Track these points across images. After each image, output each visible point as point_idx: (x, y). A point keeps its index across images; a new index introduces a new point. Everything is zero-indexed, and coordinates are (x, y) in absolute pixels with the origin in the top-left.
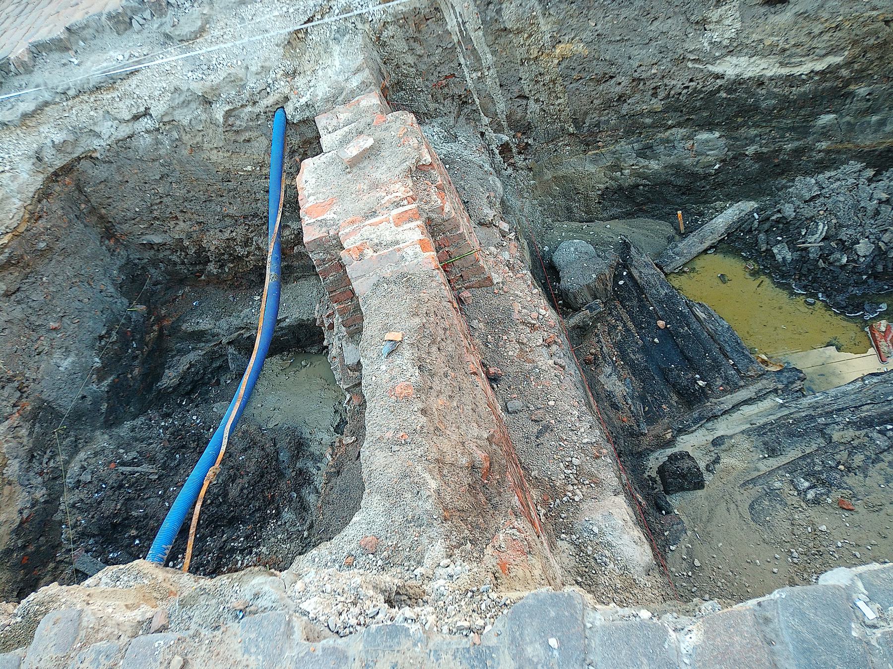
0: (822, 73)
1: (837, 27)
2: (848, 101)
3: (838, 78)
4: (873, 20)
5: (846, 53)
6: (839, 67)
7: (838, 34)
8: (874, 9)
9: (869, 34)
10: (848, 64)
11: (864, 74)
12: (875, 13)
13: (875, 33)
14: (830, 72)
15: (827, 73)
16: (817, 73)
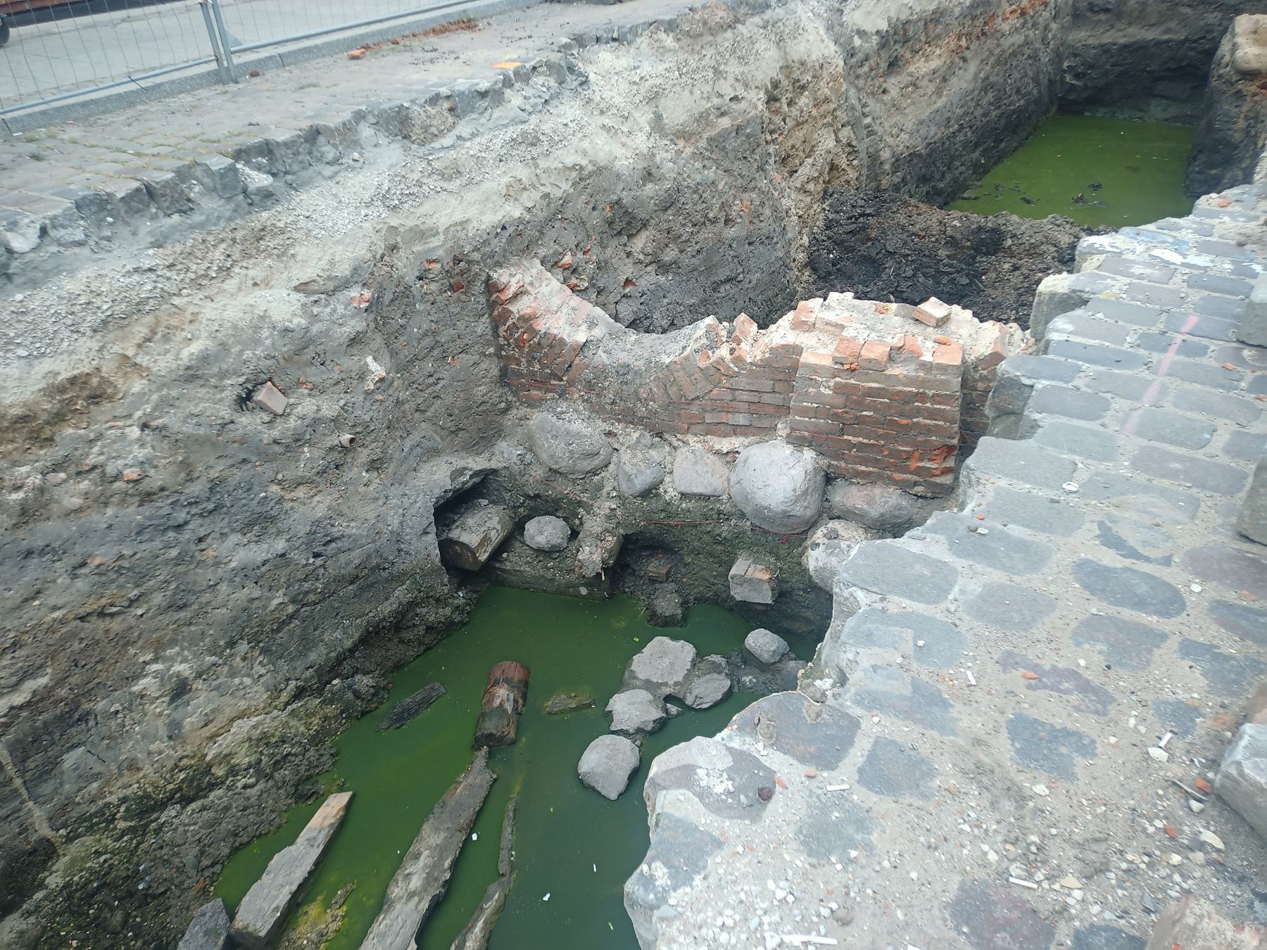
0: (28, 704)
1: (14, 644)
2: (92, 723)
3: (56, 703)
4: (63, 622)
5: (49, 670)
6: (49, 690)
7: (20, 653)
8: (55, 608)
9: (66, 639)
10: (60, 682)
11: (91, 686)
12: (57, 614)
13: (73, 635)
14: (42, 700)
15: (37, 702)
16: (21, 707)
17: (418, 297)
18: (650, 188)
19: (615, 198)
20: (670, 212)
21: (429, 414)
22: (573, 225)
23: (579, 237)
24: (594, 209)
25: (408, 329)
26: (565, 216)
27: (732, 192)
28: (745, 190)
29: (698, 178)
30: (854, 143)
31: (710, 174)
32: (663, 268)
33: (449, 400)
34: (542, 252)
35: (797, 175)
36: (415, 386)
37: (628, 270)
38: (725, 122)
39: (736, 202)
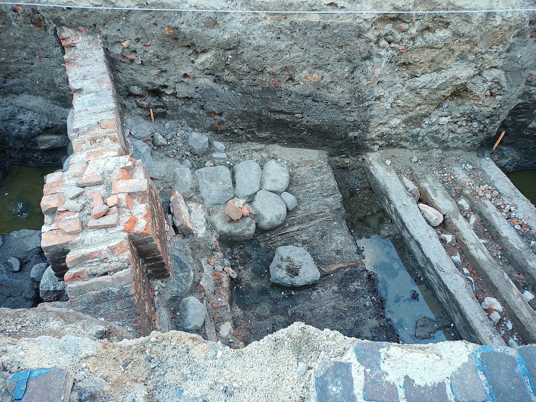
17: (12, 18)
18: (214, 32)
19: (173, 25)
20: (229, 52)
21: (28, 75)
22: (135, 27)
23: (139, 36)
24: (155, 24)
25: (8, 31)
26: (129, 20)
27: (304, 64)
28: (320, 68)
29: (263, 42)
30: (504, 84)
31: (282, 45)
32: (218, 80)
33: (39, 75)
34: (104, 32)
35: (417, 79)
36: (17, 59)
37: (189, 71)
38: (314, 17)
39: (304, 72)
